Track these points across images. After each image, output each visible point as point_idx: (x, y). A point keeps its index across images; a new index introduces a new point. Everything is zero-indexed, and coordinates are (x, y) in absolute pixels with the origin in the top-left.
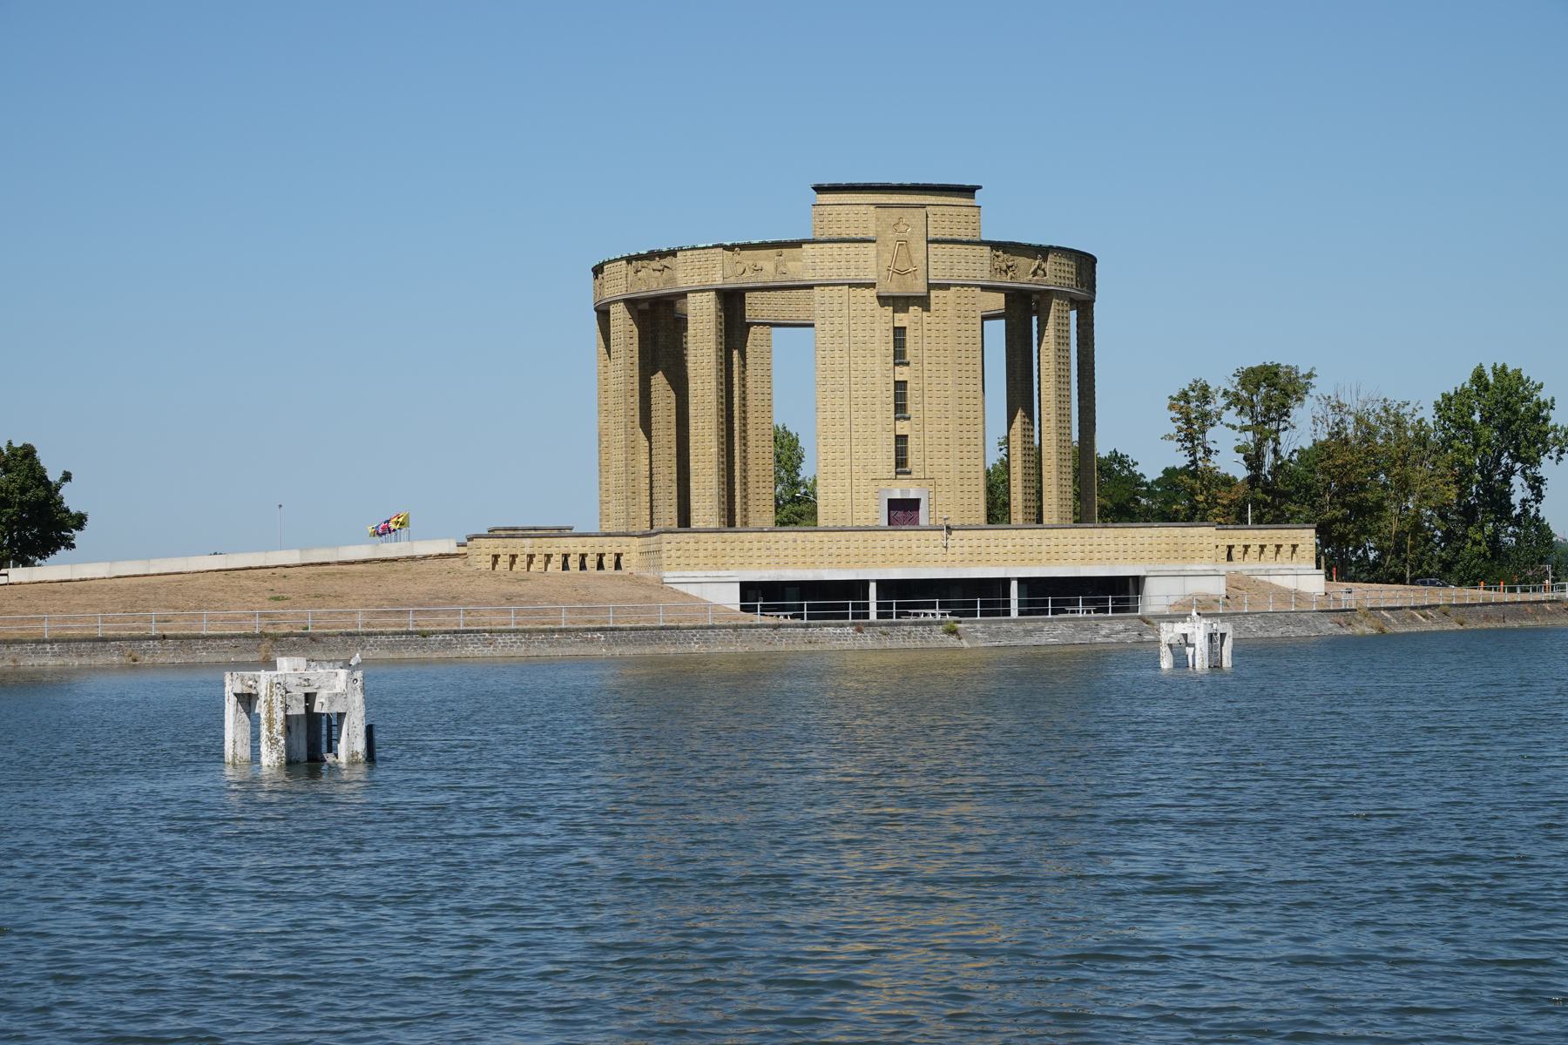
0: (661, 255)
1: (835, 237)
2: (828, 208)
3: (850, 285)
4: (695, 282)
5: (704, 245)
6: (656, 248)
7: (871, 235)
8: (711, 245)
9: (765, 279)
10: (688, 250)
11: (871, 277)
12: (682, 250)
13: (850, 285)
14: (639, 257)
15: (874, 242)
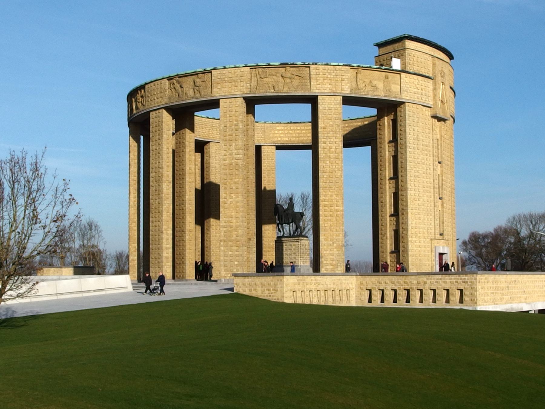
0: (293, 65)
1: (418, 72)
2: (414, 52)
3: (423, 105)
4: (327, 88)
5: (337, 64)
6: (289, 61)
7: (431, 75)
8: (342, 64)
9: (379, 94)
10: (322, 65)
11: (430, 103)
12: (316, 64)
13: (423, 105)
14: (269, 66)
15: (432, 79)
